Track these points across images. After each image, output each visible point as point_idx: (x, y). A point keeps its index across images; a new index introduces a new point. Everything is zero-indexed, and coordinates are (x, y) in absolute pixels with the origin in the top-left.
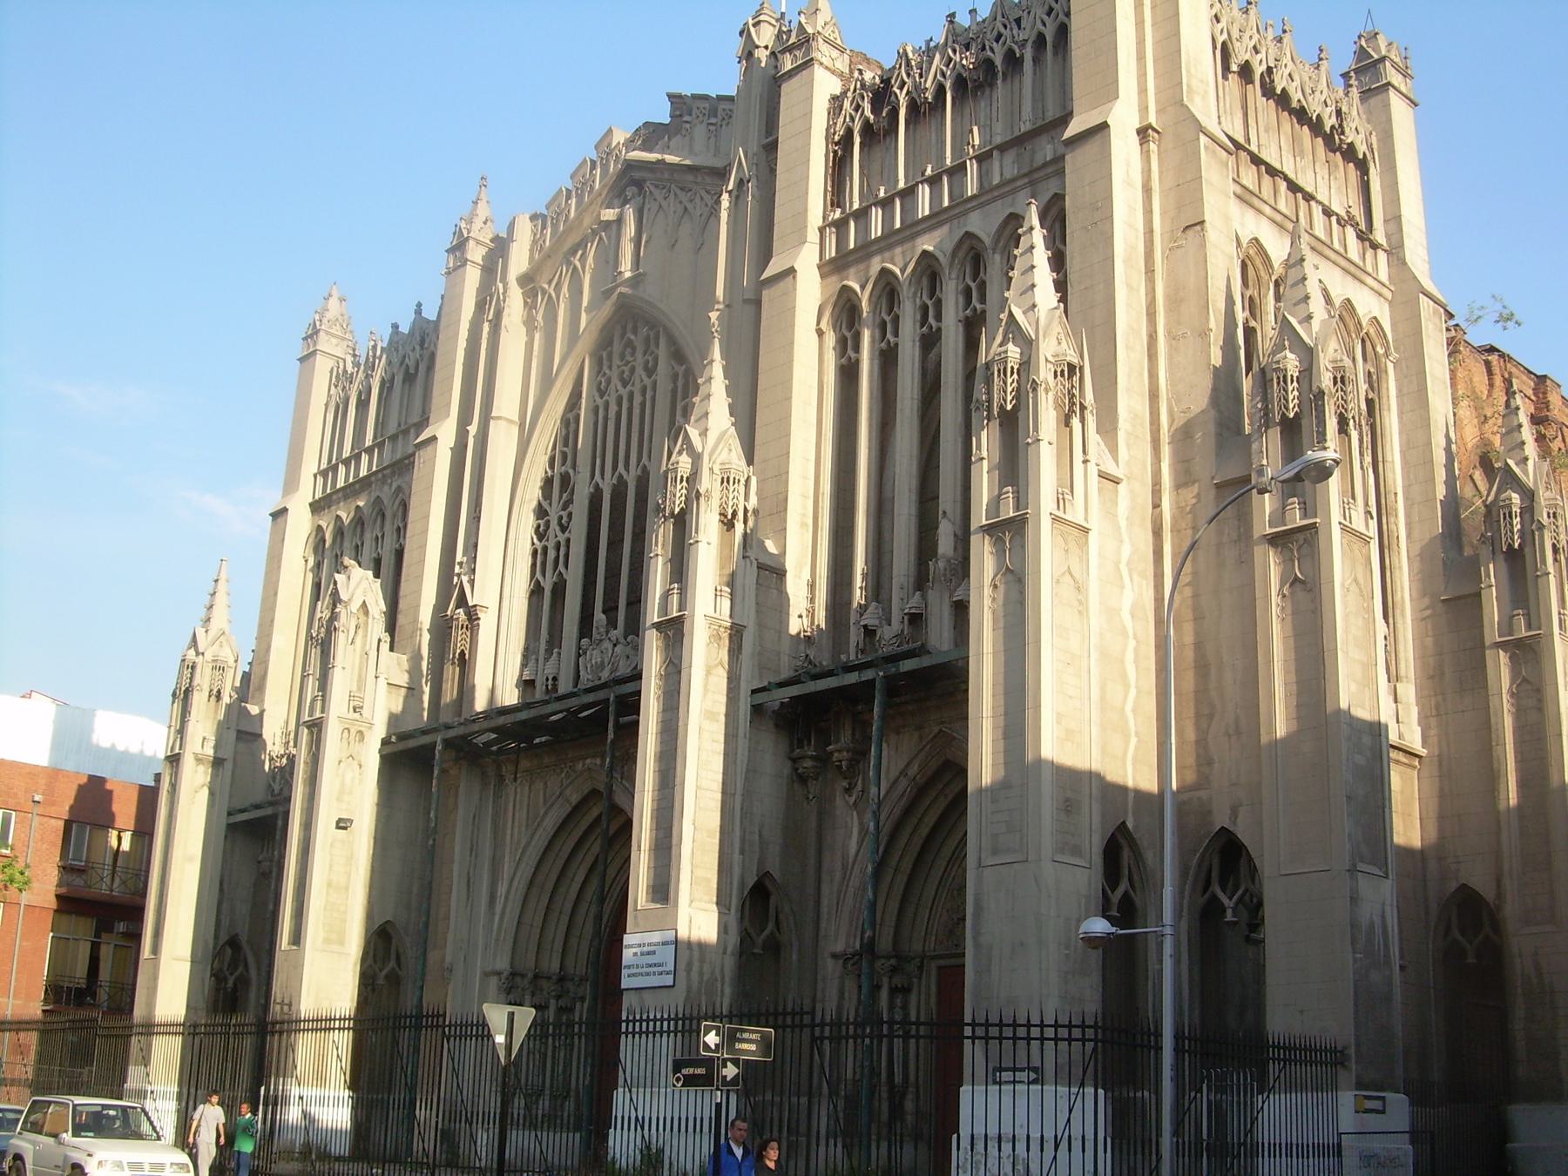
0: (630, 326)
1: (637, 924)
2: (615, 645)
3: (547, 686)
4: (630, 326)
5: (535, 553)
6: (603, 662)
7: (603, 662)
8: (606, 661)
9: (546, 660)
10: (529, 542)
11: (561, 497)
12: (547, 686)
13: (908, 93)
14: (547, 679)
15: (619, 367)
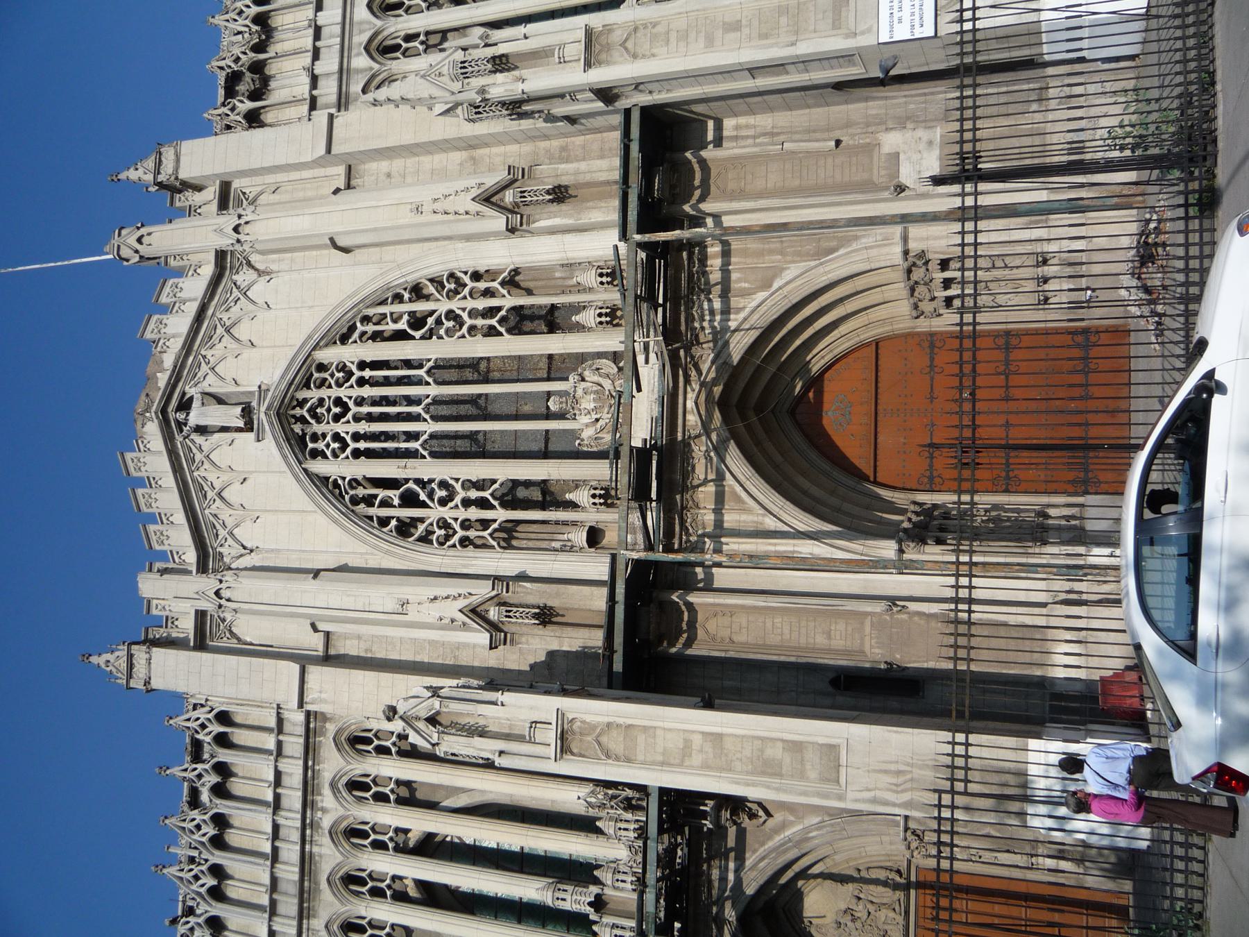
0: (298, 412)
1: (869, 30)
2: (583, 380)
3: (601, 504)
4: (298, 412)
5: (464, 542)
6: (596, 392)
7: (596, 392)
8: (596, 388)
9: (573, 505)
10: (452, 552)
11: (424, 505)
12: (601, 504)
13: (245, 53)
14: (594, 504)
15: (328, 423)
